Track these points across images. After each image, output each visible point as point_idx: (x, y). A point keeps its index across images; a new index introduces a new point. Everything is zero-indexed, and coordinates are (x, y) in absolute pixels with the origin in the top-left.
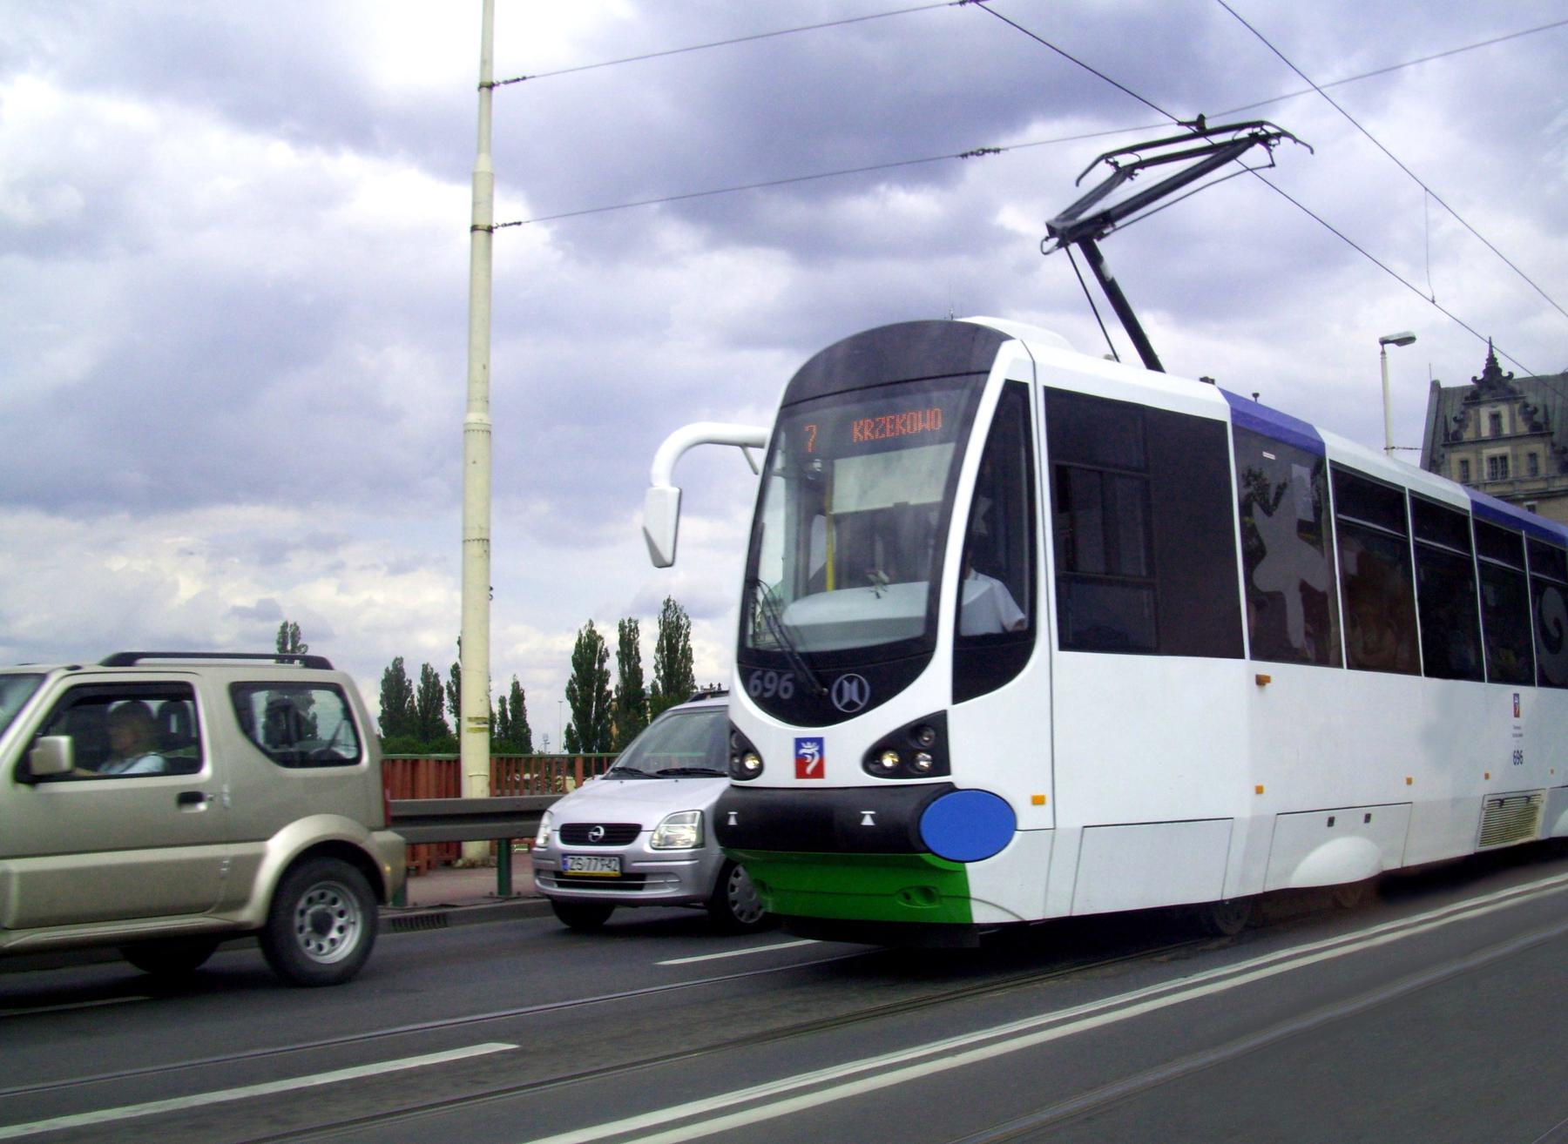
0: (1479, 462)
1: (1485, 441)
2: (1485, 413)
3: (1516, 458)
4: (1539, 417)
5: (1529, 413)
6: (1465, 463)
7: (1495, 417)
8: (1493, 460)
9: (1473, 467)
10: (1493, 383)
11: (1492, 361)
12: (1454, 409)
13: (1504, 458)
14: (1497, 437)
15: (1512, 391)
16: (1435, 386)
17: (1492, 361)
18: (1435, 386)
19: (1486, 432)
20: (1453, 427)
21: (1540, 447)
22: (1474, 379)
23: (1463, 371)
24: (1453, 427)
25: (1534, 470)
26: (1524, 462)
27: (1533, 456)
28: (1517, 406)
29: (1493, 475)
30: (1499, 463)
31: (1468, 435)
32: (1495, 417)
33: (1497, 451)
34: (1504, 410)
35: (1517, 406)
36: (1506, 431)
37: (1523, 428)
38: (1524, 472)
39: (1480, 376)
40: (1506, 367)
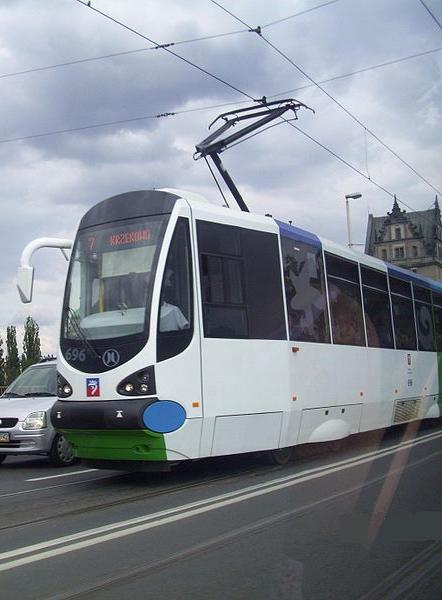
0: (391, 250)
1: (394, 241)
2: (393, 228)
3: (407, 248)
4: (417, 230)
5: (413, 228)
6: (384, 251)
7: (398, 230)
8: (397, 249)
9: (388, 252)
10: (397, 215)
11: (396, 204)
12: (379, 227)
13: (402, 249)
14: (399, 239)
15: (405, 219)
16: (371, 216)
17: (396, 204)
18: (371, 216)
19: (394, 237)
20: (379, 235)
21: (418, 243)
23: (383, 210)
24: (379, 235)
25: (416, 254)
26: (411, 249)
27: (415, 247)
28: (407, 225)
29: (397, 256)
30: (400, 251)
31: (386, 238)
32: (398, 230)
33: (399, 245)
34: (401, 227)
35: (407, 225)
36: (403, 236)
37: (410, 235)
38: (411, 255)
39: (391, 212)
40: (402, 208)
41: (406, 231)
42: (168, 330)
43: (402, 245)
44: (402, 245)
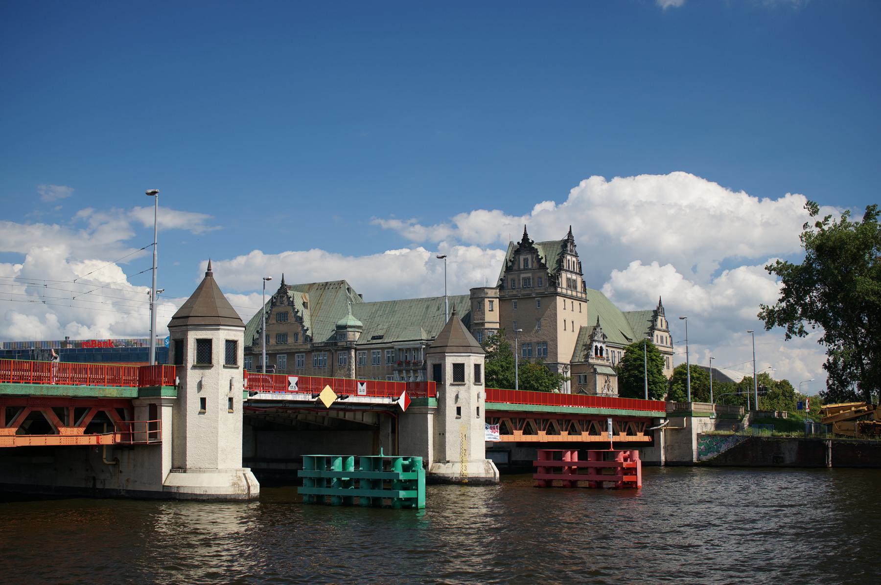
0: (519, 280)
2: (522, 258)
3: (533, 279)
7: (526, 261)
8: (524, 279)
11: (525, 235)
13: (529, 279)
14: (526, 269)
17: (525, 235)
19: (522, 267)
22: (518, 243)
27: (541, 278)
28: (535, 256)
30: (526, 280)
31: (515, 267)
32: (526, 261)
34: (529, 257)
36: (530, 267)
39: (521, 242)
40: (531, 238)
41: (533, 262)
42: (424, 296)
43: (530, 275)
44: (530, 275)
